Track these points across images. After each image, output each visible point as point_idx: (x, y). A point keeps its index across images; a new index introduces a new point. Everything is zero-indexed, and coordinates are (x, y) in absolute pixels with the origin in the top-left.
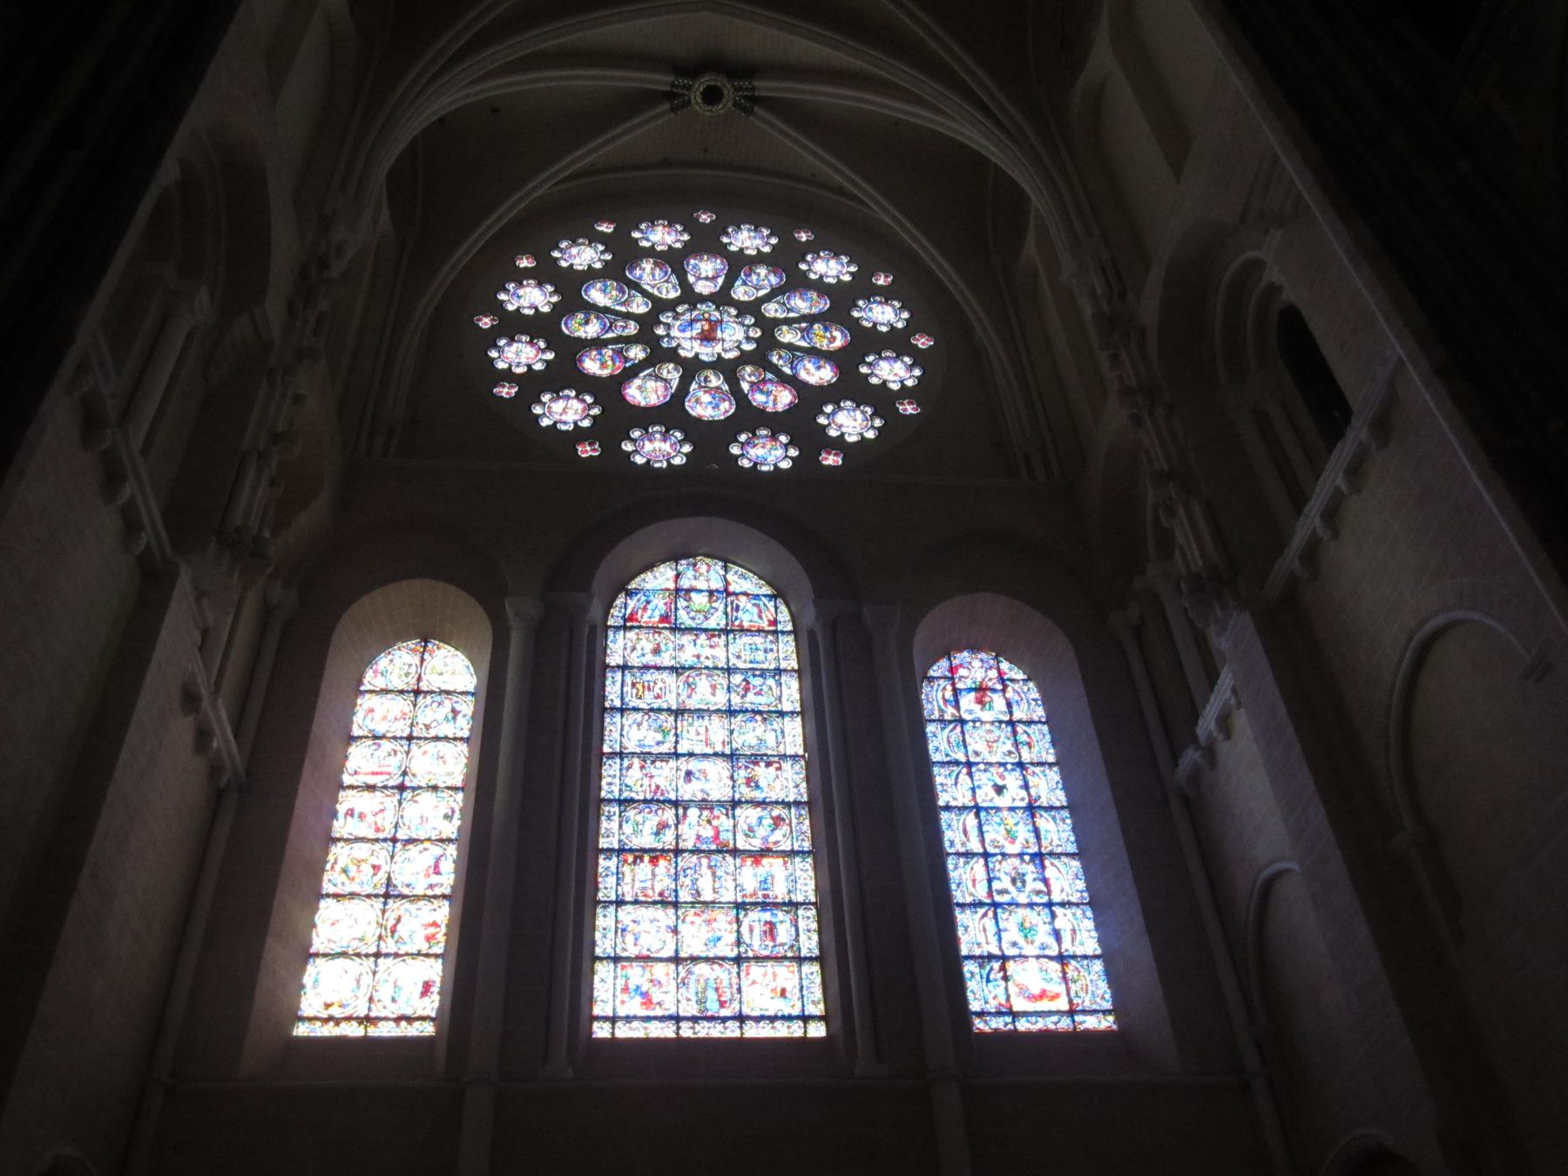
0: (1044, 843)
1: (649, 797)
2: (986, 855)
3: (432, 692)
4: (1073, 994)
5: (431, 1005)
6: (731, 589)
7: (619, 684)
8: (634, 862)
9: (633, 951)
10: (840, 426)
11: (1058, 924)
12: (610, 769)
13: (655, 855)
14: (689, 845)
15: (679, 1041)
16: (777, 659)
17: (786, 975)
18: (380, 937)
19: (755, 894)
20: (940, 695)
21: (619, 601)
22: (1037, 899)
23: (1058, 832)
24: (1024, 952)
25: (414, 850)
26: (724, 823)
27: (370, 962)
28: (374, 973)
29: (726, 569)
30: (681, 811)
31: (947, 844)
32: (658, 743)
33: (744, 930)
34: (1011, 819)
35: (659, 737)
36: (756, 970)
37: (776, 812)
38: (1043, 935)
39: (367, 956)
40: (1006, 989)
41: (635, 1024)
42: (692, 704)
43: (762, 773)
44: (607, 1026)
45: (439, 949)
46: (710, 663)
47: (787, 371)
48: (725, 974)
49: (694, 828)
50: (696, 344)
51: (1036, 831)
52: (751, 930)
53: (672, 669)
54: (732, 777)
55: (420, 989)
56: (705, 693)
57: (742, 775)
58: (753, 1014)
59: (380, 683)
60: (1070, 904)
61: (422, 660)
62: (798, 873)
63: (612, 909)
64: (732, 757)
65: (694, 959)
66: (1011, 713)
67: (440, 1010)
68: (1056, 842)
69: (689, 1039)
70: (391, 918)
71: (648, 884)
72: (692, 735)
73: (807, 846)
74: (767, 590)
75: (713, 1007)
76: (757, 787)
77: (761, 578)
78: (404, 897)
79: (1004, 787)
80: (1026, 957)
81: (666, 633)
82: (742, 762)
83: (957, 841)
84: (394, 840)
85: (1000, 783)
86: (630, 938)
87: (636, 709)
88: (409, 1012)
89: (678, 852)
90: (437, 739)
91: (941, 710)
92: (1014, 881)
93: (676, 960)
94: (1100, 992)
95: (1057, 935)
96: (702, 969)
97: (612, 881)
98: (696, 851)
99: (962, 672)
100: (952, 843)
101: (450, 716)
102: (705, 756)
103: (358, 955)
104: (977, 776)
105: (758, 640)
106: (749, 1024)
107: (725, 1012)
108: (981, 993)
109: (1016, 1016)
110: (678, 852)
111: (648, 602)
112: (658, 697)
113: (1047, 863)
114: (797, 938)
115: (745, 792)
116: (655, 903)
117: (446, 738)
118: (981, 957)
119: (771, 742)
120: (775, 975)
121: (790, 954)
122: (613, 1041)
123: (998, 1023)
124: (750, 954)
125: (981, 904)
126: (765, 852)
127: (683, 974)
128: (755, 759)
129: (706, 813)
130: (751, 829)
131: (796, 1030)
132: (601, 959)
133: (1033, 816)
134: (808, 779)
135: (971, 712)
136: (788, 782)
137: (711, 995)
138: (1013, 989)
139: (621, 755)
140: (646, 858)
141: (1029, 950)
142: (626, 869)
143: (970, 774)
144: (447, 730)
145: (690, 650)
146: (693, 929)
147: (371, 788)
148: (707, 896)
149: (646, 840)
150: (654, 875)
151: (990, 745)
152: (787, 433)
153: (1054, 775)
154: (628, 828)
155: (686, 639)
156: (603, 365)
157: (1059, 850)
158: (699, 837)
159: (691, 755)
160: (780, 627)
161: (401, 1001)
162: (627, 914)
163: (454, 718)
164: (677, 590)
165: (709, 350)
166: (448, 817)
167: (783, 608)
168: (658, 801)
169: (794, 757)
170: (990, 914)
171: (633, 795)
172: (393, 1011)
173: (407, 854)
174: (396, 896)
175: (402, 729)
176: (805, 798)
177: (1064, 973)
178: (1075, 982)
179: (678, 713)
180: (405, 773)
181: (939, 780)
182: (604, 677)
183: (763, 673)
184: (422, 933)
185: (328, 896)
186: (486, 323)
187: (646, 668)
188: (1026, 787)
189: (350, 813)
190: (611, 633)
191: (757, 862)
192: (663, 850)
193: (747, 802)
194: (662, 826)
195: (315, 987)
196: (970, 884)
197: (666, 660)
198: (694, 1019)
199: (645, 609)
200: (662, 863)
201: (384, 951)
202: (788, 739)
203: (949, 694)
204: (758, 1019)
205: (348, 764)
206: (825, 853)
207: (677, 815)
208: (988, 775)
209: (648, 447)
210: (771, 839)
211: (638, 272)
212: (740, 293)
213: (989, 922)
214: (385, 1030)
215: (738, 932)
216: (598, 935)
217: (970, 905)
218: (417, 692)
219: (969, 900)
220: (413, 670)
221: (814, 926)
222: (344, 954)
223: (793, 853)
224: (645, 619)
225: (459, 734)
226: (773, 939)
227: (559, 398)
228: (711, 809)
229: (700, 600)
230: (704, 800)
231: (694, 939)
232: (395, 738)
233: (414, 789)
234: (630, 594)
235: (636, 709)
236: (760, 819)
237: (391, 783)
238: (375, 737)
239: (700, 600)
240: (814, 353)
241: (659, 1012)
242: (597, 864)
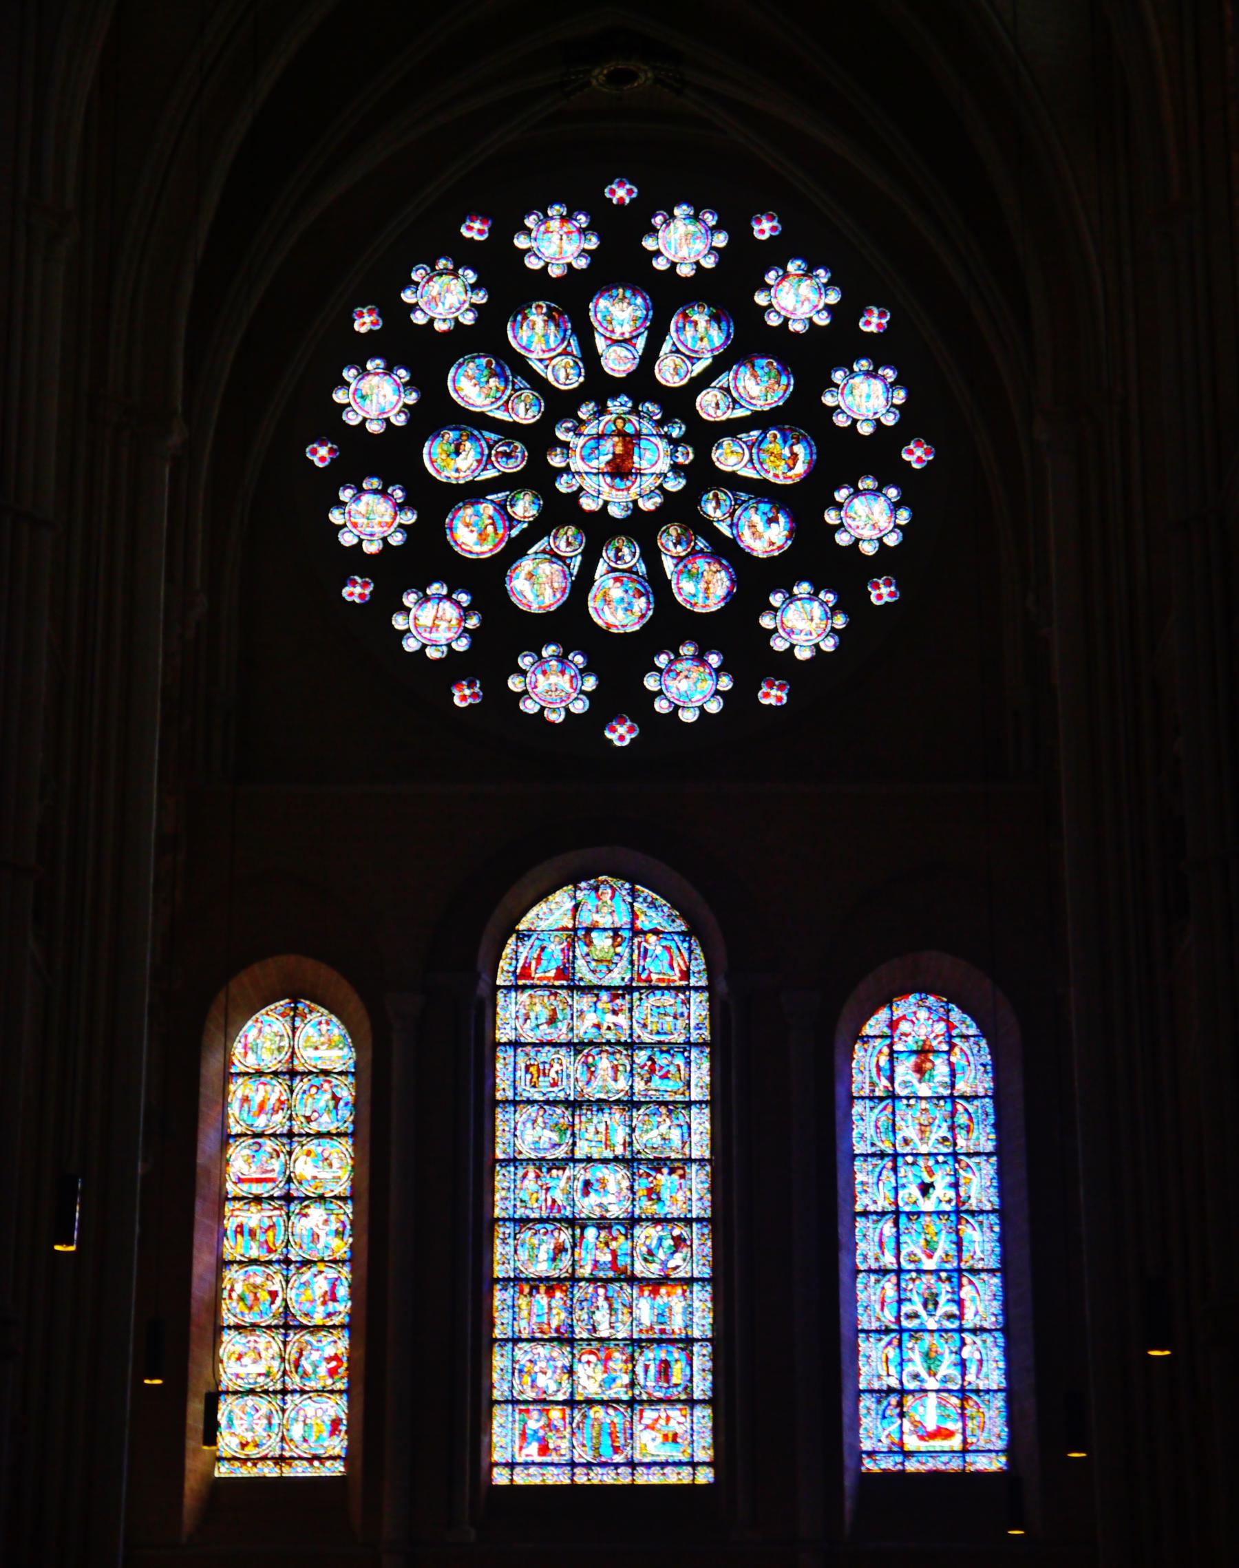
0: (965, 1255)
1: (545, 1215)
2: (899, 1272)
3: (310, 1073)
4: (968, 1432)
5: (338, 1445)
6: (639, 924)
7: (511, 1068)
8: (531, 1294)
9: (530, 1395)
10: (791, 632)
11: (966, 1353)
12: (503, 1178)
13: (551, 1285)
14: (586, 1271)
15: (573, 1487)
16: (687, 1027)
17: (677, 1419)
18: (285, 1373)
19: (652, 1328)
20: (874, 1060)
21: (508, 951)
22: (948, 1325)
23: (981, 1242)
24: (927, 1386)
25: (307, 1275)
26: (621, 1245)
27: (278, 1405)
28: (284, 1411)
29: (633, 894)
30: (578, 1231)
31: (859, 1260)
32: (555, 1146)
33: (639, 1370)
34: (934, 1225)
35: (555, 1137)
36: (650, 1415)
37: (676, 1232)
38: (946, 1367)
39: (275, 1392)
40: (901, 1425)
41: (533, 1470)
42: (594, 1092)
43: (665, 1180)
44: (506, 1471)
45: (341, 1385)
46: (611, 1036)
47: (724, 529)
48: (616, 1417)
49: (593, 1252)
50: (604, 483)
51: (959, 1243)
52: (646, 1368)
53: (569, 1044)
54: (631, 1188)
55: (326, 1429)
56: (608, 1078)
57: (642, 1185)
58: (646, 1460)
59: (252, 1061)
60: (983, 1330)
61: (294, 1029)
62: (696, 1304)
63: (510, 1345)
64: (630, 1162)
65: (590, 1402)
66: (953, 1086)
67: (348, 1449)
68: (979, 1255)
69: (583, 1486)
70: (292, 1351)
71: (545, 1319)
72: (591, 1135)
73: (706, 1272)
74: (680, 926)
75: (607, 1453)
76: (659, 1199)
77: (674, 906)
78: (303, 1327)
79: (932, 1185)
80: (926, 1391)
81: (563, 993)
82: (643, 1169)
83: (870, 1254)
84: (287, 1262)
85: (928, 1180)
86: (527, 1379)
87: (530, 1102)
88: (320, 1452)
89: (574, 1279)
90: (319, 1135)
91: (873, 1084)
92: (925, 1305)
93: (571, 1403)
94: (997, 1430)
95: (963, 1364)
96: (598, 1412)
97: (508, 1315)
98: (593, 1280)
99: (904, 1027)
100: (865, 1257)
101: (331, 1103)
102: (605, 1161)
103: (266, 1392)
104: (902, 1171)
105: (668, 998)
106: (640, 1469)
107: (618, 1458)
108: (875, 1432)
109: (908, 1454)
110: (574, 1279)
111: (543, 949)
112: (554, 1084)
113: (965, 1281)
114: (691, 1381)
115: (645, 1207)
116: (551, 1340)
117: (329, 1135)
118: (879, 1391)
119: (676, 1141)
120: (668, 1418)
121: (683, 1397)
122: (512, 1488)
123: (888, 1464)
124: (645, 1397)
125: (887, 1331)
126: (664, 1281)
127: (578, 1417)
128: (658, 1164)
129: (603, 1234)
130: (650, 1253)
131: (682, 1477)
132: (499, 1402)
133: (959, 1222)
134: (713, 1190)
135: (906, 1084)
136: (690, 1193)
137: (606, 1441)
138: (907, 1426)
139: (513, 1161)
140: (542, 1289)
141: (931, 1384)
142: (523, 1302)
143: (895, 1170)
144: (327, 1123)
145: (591, 1017)
146: (590, 1371)
147: (258, 1199)
148: (604, 1332)
149: (542, 1267)
150: (550, 1308)
151: (923, 1129)
152: (721, 650)
153: (988, 1168)
154: (523, 1254)
155: (583, 1002)
156: (482, 537)
157: (980, 1265)
158: (596, 1262)
159: (589, 1160)
160: (693, 982)
161: (312, 1440)
162: (523, 1354)
163: (336, 1107)
164: (575, 929)
165: (622, 497)
166: (339, 1234)
167: (698, 951)
168: (555, 1219)
169: (701, 1161)
170: (895, 1342)
171: (528, 1212)
172: (304, 1450)
173: (304, 1279)
174: (295, 1327)
175: (278, 1122)
176: (708, 1214)
177: (963, 1408)
178: (972, 1418)
179: (573, 1105)
180: (289, 1180)
181: (860, 1177)
182: (494, 1059)
183: (667, 1048)
184: (323, 1370)
185: (229, 1327)
186: (321, 455)
187: (542, 1044)
188: (955, 1185)
189: (240, 1229)
190: (500, 996)
191: (655, 1292)
192: (558, 1279)
193: (647, 1219)
194: (559, 1250)
195: (230, 1426)
196: (878, 1307)
197: (561, 1033)
198: (588, 1465)
199: (539, 959)
200: (558, 1294)
201: (290, 1387)
202: (695, 1138)
203: (884, 1061)
204: (649, 1465)
205: (231, 1170)
206: (723, 1283)
207: (573, 1236)
208: (915, 1168)
209: (543, 683)
210: (671, 1264)
211: (524, 334)
212: (669, 372)
213: (892, 1353)
214: (300, 1470)
215: (633, 1372)
216: (495, 1376)
217: (877, 1331)
218: (293, 1073)
219: (875, 1325)
220: (285, 1043)
221: (709, 1365)
222: (251, 1392)
223: (690, 1281)
224: (537, 974)
225: (342, 1129)
226: (668, 1380)
227: (427, 599)
228: (610, 1228)
229: (602, 942)
230: (603, 1218)
231: (590, 1380)
232: (274, 1135)
233: (302, 1199)
234: (522, 937)
235: (530, 1102)
236: (660, 1239)
237: (277, 1193)
238: (255, 1135)
239: (602, 942)
240: (761, 490)
241: (554, 1458)
242: (492, 1297)
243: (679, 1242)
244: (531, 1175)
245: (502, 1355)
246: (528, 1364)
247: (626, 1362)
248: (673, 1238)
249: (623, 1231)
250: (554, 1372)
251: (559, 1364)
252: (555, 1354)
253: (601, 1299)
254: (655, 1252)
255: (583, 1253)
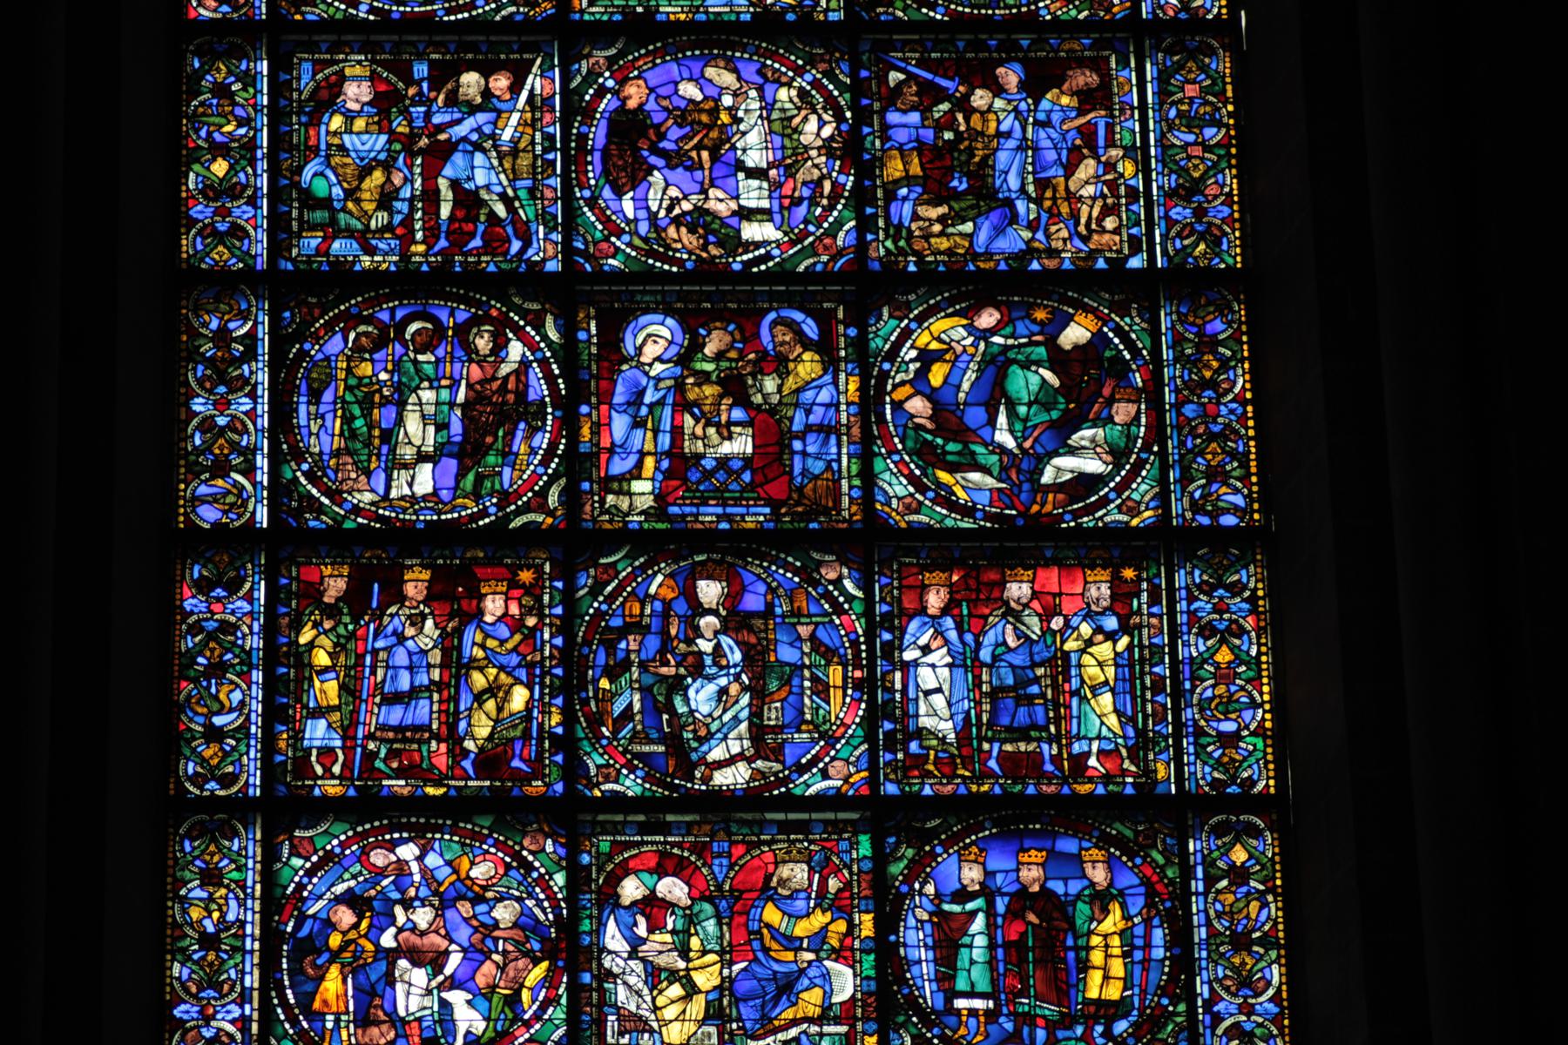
33: (915, 939)
76: (986, 197)
193: (928, 279)
207: (568, 352)
236: (996, 367)
243: (1084, 385)
244: (357, 93)
245: (211, 877)
246: (345, 916)
247: (840, 906)
248: (1058, 359)
249: (811, 329)
250: (476, 954)
251: (504, 913)
252: (481, 871)
253: (708, 622)
254: (975, 416)
255: (620, 424)
